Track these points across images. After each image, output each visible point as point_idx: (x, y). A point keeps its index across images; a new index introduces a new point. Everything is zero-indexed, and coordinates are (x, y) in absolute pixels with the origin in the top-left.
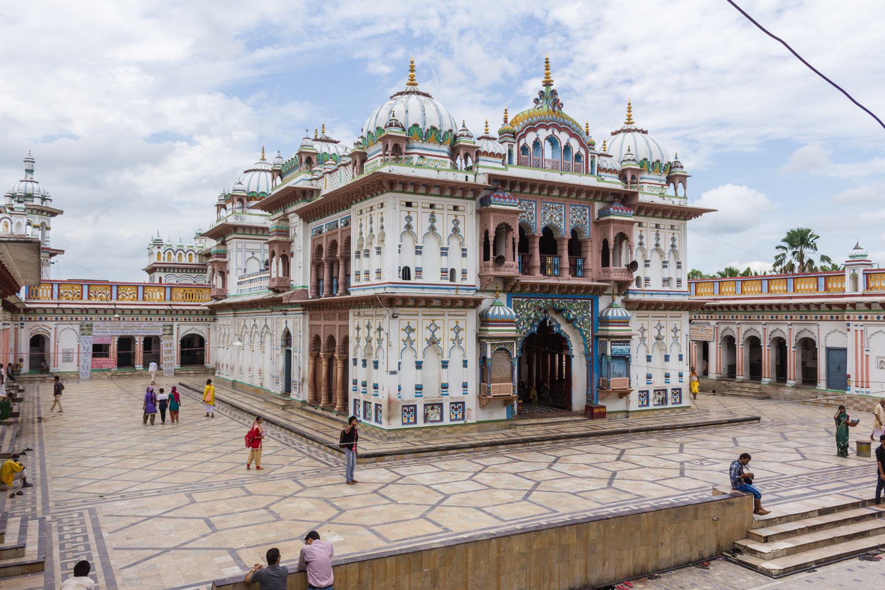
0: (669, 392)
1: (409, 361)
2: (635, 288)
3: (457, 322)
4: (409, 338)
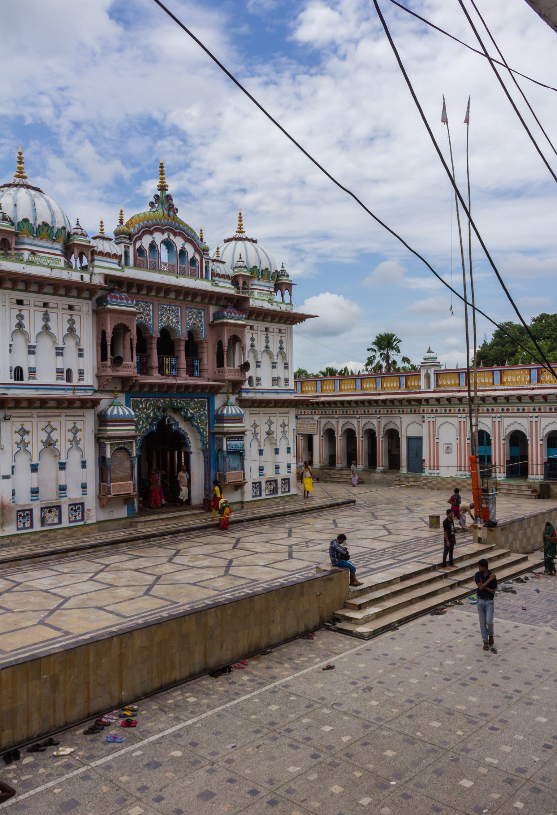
0: (279, 482)
1: (23, 463)
2: (248, 387)
3: (75, 423)
4: (22, 440)
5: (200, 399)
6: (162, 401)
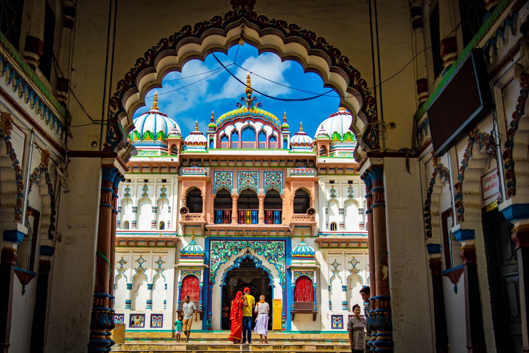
3: (160, 257)
4: (122, 267)
5: (277, 242)
6: (240, 243)
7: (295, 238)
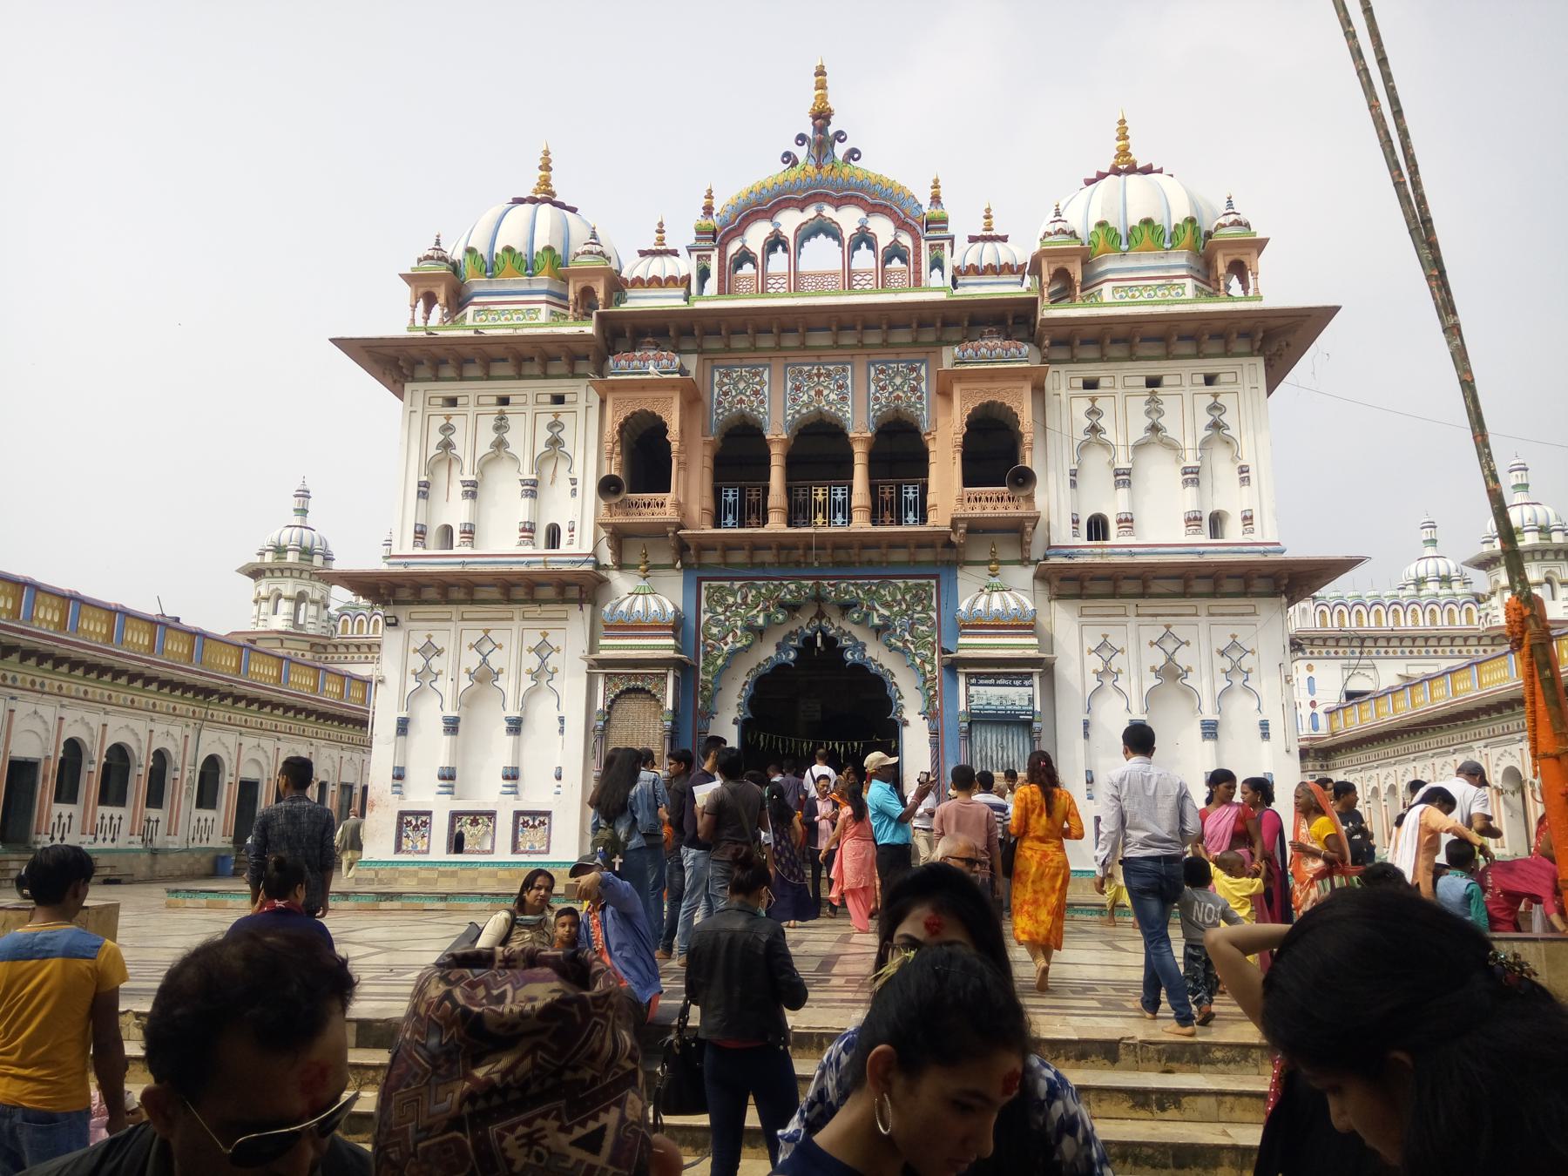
1: (430, 717)
3: (545, 635)
4: (427, 667)
5: (911, 582)
7: (968, 569)
